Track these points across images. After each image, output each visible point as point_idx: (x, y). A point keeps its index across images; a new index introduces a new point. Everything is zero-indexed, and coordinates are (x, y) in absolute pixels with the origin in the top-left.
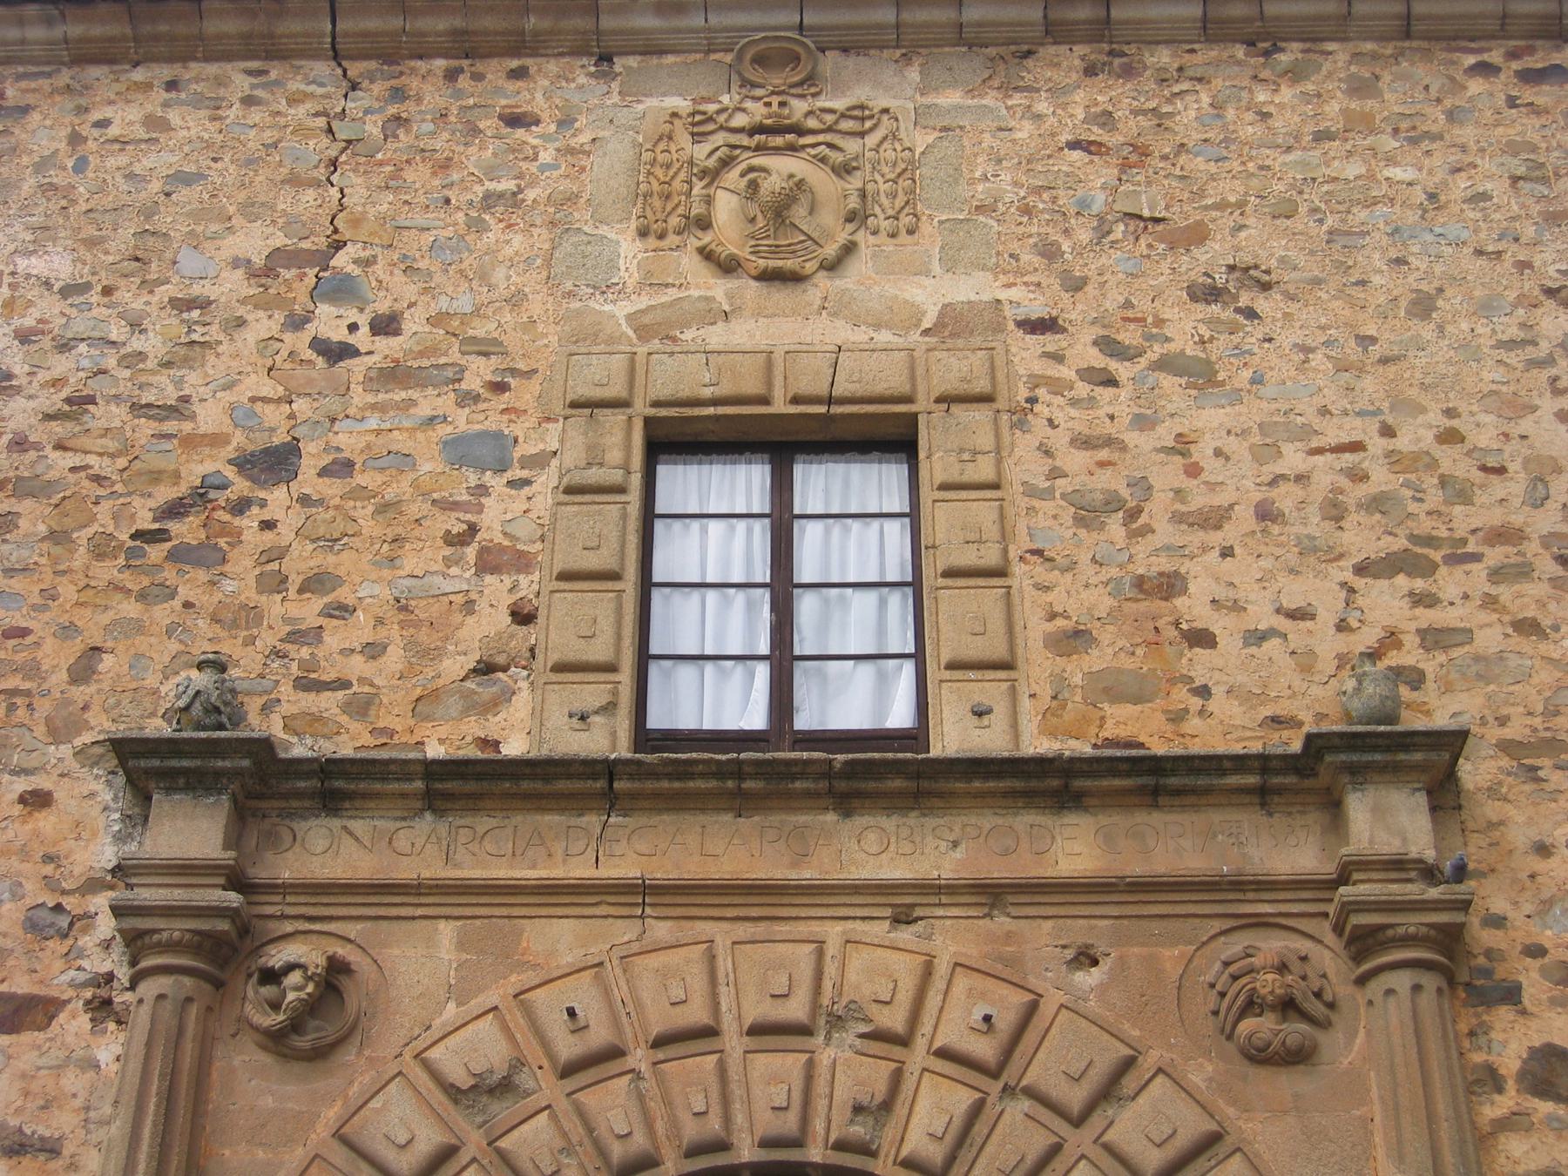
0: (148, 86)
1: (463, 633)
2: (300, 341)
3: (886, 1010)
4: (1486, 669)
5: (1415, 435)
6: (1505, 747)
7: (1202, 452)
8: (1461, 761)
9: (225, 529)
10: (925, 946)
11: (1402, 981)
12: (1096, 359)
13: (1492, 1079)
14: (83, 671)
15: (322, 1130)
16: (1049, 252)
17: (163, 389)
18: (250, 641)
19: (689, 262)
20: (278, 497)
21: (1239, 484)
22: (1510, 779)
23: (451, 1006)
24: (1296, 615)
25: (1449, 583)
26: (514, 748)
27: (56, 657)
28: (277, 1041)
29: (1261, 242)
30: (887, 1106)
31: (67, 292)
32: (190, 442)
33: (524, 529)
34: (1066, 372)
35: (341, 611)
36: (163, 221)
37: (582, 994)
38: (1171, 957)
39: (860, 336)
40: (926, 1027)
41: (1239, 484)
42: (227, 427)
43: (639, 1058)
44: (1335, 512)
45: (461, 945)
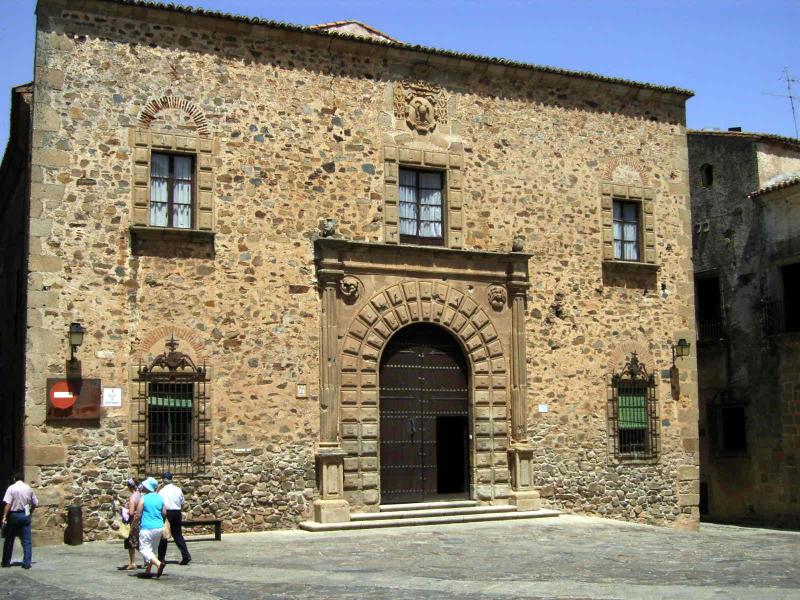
0: (286, 51)
2: (331, 135)
4: (535, 237)
5: (529, 186)
6: (537, 253)
7: (494, 186)
9: (322, 183)
11: (518, 298)
12: (478, 161)
13: (527, 314)
14: (301, 216)
15: (356, 315)
16: (471, 131)
17: (305, 145)
19: (405, 124)
20: (331, 175)
21: (499, 194)
24: (507, 223)
25: (532, 218)
26: (380, 241)
27: (295, 212)
29: (509, 135)
31: (280, 113)
32: (313, 159)
33: (379, 189)
34: (472, 163)
35: (347, 205)
36: (298, 95)
39: (437, 148)
41: (499, 194)
42: (319, 156)
43: (405, 302)
44: (515, 201)
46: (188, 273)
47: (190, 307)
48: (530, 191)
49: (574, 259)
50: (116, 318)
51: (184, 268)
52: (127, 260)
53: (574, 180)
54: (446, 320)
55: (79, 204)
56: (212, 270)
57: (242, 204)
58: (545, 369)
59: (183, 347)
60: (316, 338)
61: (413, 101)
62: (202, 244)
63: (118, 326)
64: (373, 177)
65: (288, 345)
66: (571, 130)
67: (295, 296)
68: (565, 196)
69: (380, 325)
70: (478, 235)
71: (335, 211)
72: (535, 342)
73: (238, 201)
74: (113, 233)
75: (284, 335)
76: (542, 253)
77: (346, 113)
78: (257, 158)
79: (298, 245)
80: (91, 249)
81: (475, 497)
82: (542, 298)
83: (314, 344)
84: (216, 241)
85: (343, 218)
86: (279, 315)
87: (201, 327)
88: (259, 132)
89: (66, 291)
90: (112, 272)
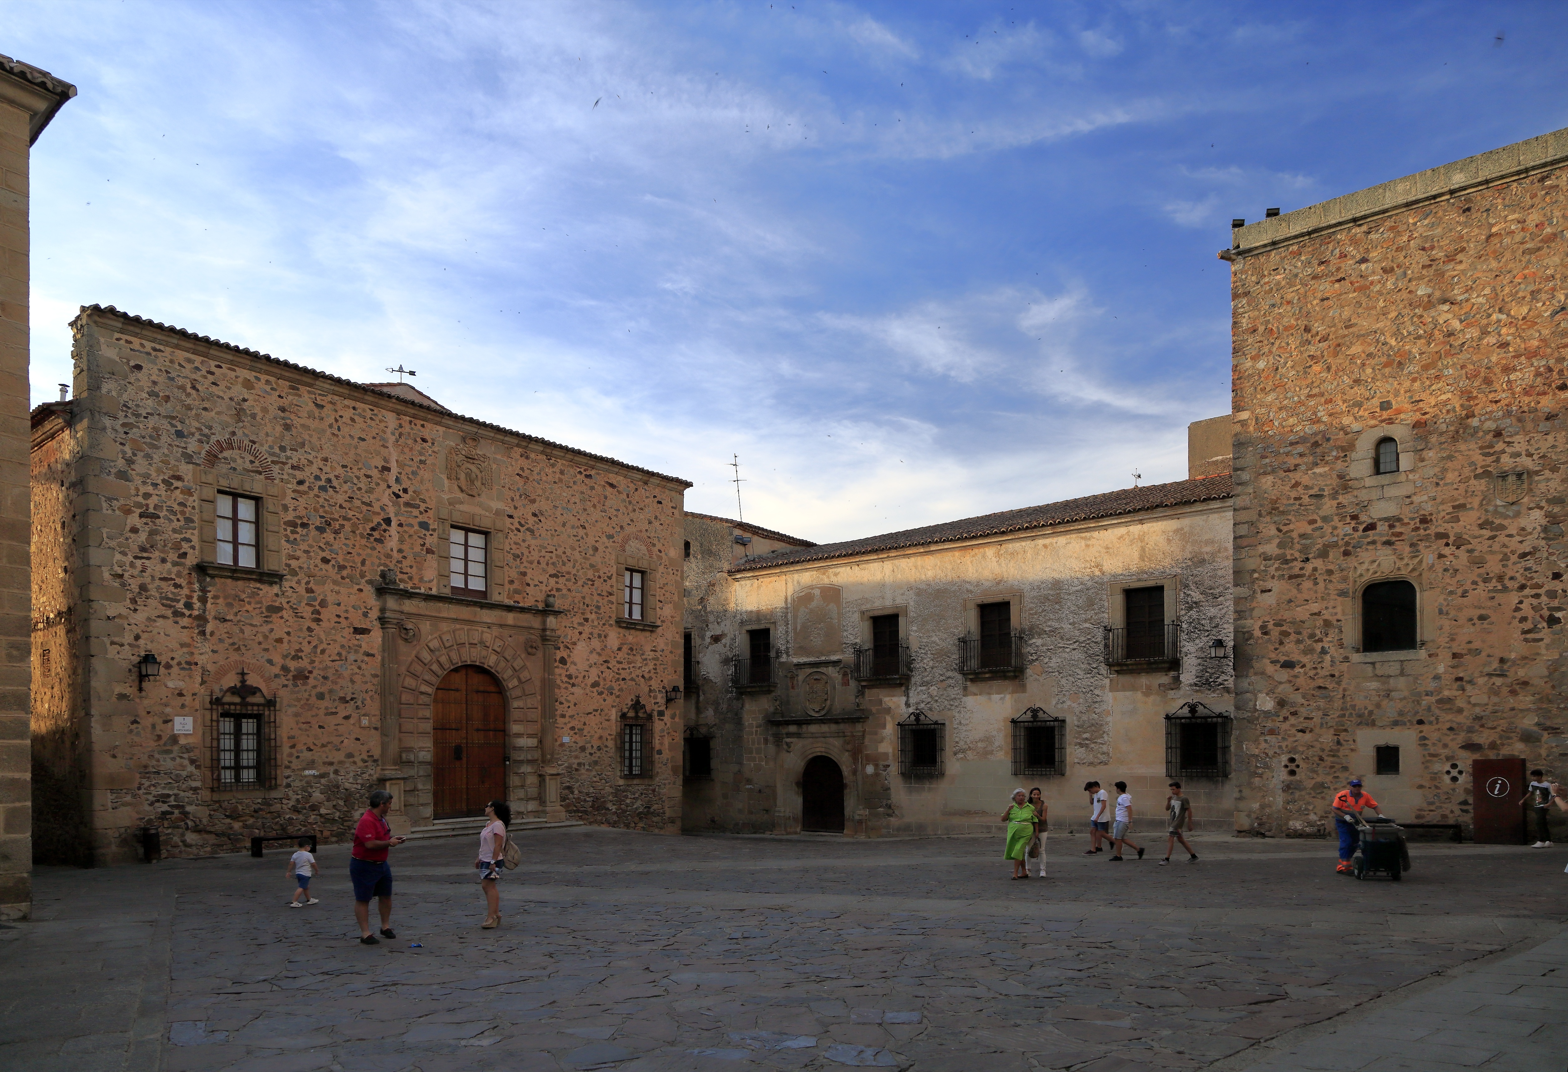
9: (382, 536)
14: (363, 563)
19: (456, 488)
27: (358, 560)
28: (406, 640)
35: (404, 557)
39: (483, 512)
41: (535, 555)
42: (379, 510)
46: (258, 611)
47: (260, 643)
48: (557, 556)
49: (594, 616)
50: (185, 650)
51: (253, 605)
52: (195, 595)
53: (596, 549)
54: (491, 664)
55: (143, 537)
56: (279, 609)
57: (307, 548)
59: (253, 680)
60: (377, 676)
61: (463, 467)
62: (271, 584)
63: (188, 658)
64: (428, 534)
65: (352, 681)
66: (594, 506)
67: (358, 637)
68: (588, 563)
69: (435, 667)
71: (394, 562)
73: (304, 547)
74: (181, 568)
75: (349, 672)
77: (404, 473)
78: (323, 506)
79: (361, 590)
80: (157, 582)
84: (285, 583)
86: (344, 653)
87: (270, 662)
88: (323, 483)
89: (133, 621)
90: (180, 606)
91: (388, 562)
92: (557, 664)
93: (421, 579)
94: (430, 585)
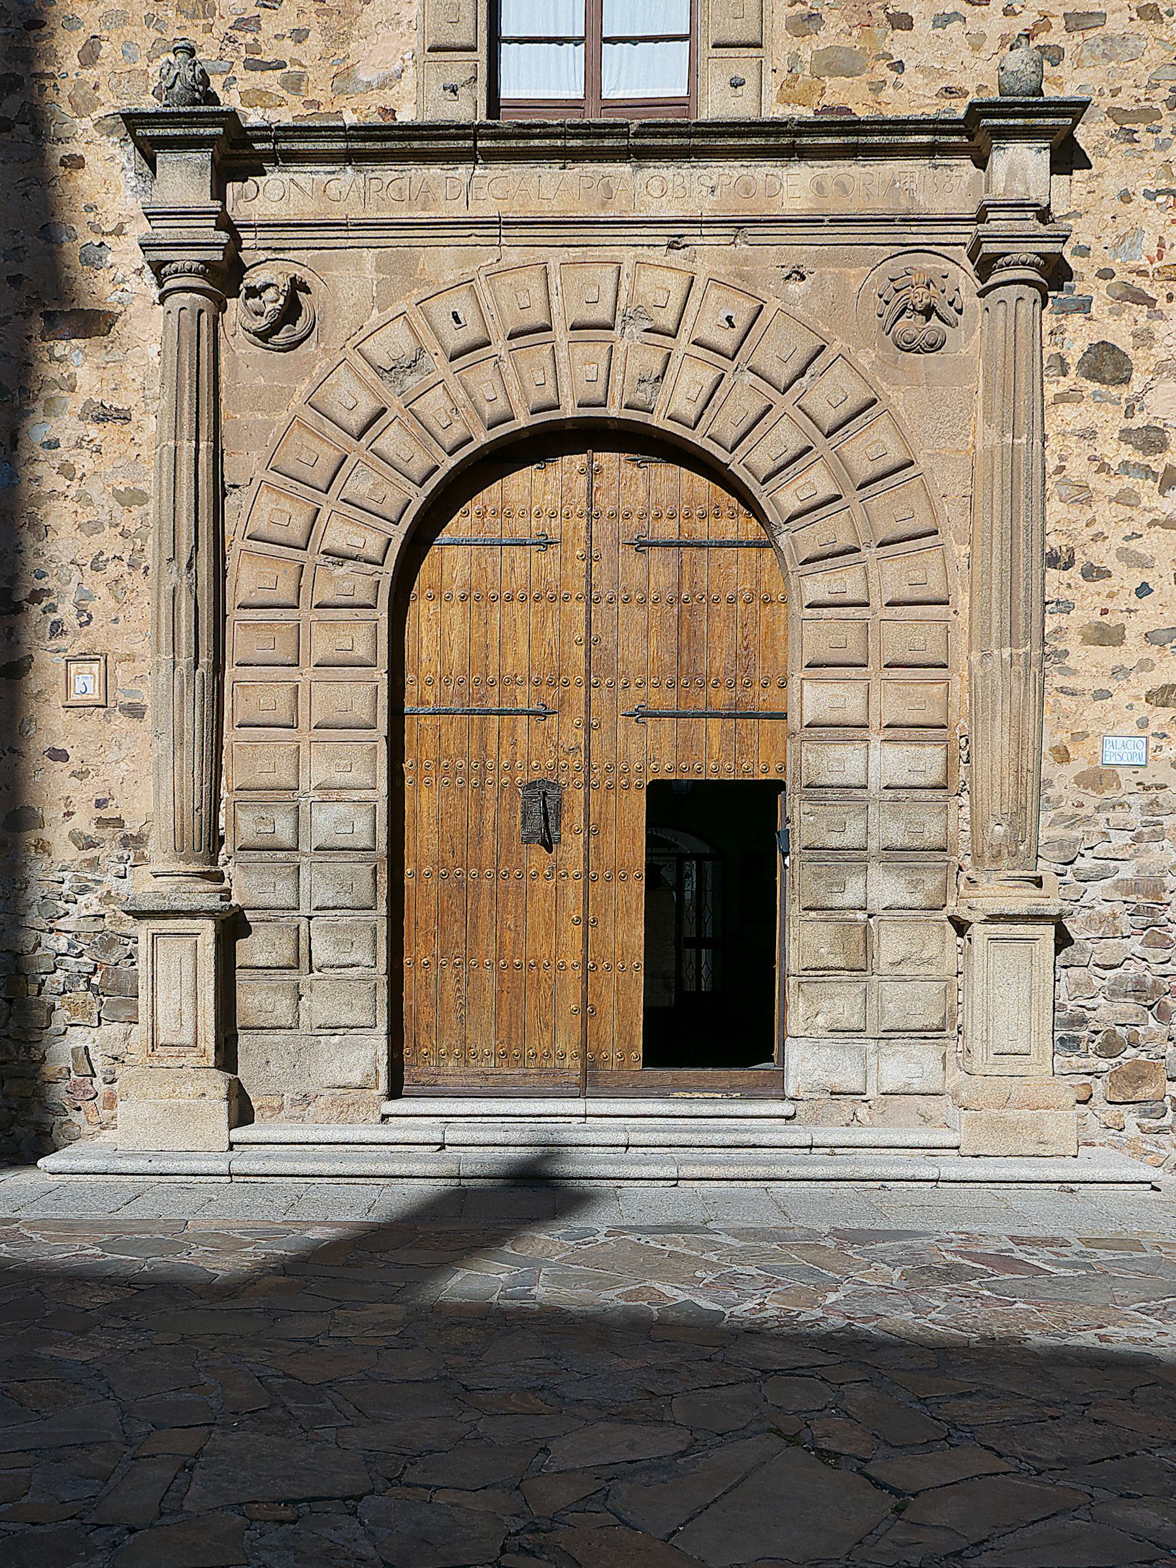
1: (363, 19)
3: (662, 312)
6: (1112, 113)
8: (1079, 125)
10: (689, 266)
15: (297, 401)
18: (209, 29)
22: (1113, 140)
23: (375, 311)
26: (406, 116)
30: (660, 378)
37: (462, 303)
38: (855, 277)
40: (687, 325)
43: (500, 346)
45: (378, 269)
58: (1143, 590)
60: (140, 498)
70: (836, 64)
71: (221, 27)
72: (1096, 481)
76: (1149, 115)
81: (790, 1091)
82: (1141, 298)
83: (129, 519)
85: (254, 48)
91: (194, 35)
92: (1066, 383)
93: (344, 78)
94: (386, 98)
